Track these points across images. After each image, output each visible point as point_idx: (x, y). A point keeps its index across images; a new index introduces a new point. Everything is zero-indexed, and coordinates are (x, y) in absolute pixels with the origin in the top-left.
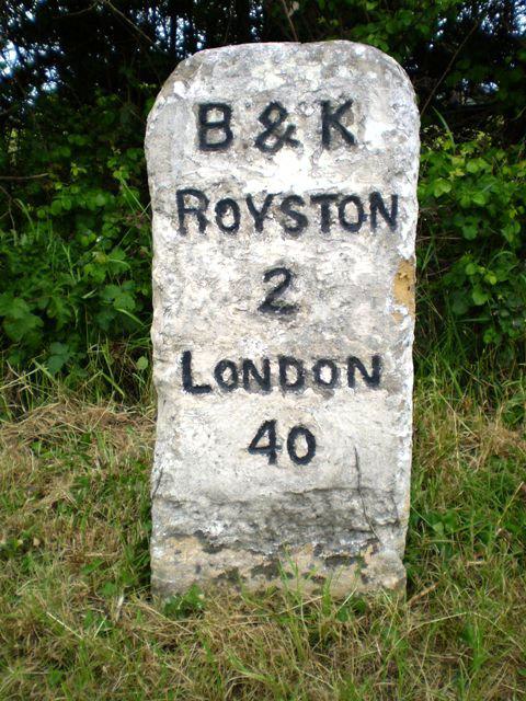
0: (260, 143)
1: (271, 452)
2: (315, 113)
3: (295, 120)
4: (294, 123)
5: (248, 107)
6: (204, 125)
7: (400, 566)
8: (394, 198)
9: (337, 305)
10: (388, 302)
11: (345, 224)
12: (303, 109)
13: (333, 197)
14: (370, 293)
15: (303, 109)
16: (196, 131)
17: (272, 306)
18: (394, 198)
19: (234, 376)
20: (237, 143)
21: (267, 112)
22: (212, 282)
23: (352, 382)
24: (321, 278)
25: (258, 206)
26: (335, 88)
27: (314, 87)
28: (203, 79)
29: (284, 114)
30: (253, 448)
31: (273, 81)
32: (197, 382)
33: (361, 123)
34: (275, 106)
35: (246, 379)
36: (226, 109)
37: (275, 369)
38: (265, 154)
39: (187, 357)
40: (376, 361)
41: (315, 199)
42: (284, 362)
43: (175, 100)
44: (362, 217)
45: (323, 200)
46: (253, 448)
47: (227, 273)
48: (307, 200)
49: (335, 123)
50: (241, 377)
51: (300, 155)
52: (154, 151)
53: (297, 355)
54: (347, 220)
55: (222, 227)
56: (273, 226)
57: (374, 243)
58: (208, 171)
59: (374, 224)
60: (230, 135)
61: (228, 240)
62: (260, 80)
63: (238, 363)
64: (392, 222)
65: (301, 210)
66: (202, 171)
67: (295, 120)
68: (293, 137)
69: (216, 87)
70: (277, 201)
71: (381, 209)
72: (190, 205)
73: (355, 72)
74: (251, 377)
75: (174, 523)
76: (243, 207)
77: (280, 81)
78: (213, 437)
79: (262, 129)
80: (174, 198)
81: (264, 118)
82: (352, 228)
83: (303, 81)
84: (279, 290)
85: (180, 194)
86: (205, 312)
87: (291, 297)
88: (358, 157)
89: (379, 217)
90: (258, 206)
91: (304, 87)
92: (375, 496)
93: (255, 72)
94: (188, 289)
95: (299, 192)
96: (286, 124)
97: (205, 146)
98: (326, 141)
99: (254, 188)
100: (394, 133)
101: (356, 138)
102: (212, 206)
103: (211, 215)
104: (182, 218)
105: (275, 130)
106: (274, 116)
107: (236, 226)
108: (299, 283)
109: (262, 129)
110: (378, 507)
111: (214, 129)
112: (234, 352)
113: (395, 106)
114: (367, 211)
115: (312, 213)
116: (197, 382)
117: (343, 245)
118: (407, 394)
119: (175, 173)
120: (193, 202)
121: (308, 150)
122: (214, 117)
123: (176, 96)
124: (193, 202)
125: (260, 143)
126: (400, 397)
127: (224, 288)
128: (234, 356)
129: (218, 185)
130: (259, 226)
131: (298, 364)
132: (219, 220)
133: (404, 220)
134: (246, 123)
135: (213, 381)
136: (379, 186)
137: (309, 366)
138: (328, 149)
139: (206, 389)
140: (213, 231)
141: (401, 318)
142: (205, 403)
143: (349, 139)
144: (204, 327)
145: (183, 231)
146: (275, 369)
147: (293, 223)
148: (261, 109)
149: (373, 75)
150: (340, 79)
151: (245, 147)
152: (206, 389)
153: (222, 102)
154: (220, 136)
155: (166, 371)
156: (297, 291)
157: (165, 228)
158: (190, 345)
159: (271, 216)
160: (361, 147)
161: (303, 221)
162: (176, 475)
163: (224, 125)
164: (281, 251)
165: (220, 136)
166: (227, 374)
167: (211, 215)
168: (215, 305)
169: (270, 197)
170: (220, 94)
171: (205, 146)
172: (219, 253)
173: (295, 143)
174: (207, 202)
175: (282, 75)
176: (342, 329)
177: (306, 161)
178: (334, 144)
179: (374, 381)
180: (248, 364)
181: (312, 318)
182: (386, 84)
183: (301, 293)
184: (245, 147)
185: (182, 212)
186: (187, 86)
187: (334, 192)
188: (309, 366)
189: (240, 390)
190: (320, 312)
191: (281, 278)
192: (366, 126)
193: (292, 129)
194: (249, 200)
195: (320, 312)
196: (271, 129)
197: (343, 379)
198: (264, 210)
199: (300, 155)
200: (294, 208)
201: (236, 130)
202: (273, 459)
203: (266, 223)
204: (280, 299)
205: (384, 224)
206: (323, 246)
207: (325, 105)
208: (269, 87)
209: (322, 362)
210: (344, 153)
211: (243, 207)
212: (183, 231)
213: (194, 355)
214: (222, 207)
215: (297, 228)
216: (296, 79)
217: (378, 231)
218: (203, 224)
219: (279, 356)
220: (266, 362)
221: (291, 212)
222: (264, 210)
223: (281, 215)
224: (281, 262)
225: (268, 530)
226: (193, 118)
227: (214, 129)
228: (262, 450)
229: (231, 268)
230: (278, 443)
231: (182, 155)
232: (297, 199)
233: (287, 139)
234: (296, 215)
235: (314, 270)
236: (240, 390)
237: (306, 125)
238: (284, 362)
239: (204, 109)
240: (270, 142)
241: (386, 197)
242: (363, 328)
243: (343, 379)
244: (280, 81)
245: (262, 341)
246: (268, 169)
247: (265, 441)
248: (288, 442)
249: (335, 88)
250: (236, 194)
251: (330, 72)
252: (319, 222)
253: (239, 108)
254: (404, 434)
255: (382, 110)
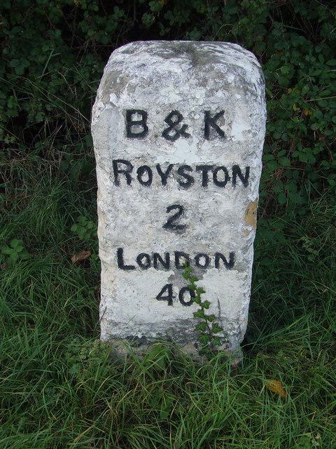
0: (165, 134)
1: (170, 300)
2: (200, 118)
3: (187, 121)
4: (186, 123)
5: (158, 113)
6: (129, 122)
7: (241, 354)
8: (248, 169)
9: (210, 226)
10: (241, 225)
11: (216, 182)
12: (193, 115)
13: (209, 167)
14: (230, 220)
15: (193, 115)
16: (124, 126)
17: (170, 225)
18: (248, 169)
19: (148, 261)
20: (150, 135)
21: (171, 116)
22: (135, 212)
23: (217, 265)
24: (201, 211)
25: (164, 170)
26: (214, 103)
27: (201, 102)
28: (129, 95)
29: (180, 118)
30: (159, 298)
31: (174, 98)
32: (126, 264)
33: (230, 125)
34: (175, 113)
35: (155, 262)
36: (144, 114)
37: (172, 258)
38: (168, 141)
39: (120, 252)
40: (232, 255)
41: (199, 168)
42: (178, 255)
43: (111, 107)
44: (227, 178)
45: (204, 169)
46: (159, 298)
47: (144, 207)
48: (194, 169)
49: (212, 125)
50: (152, 262)
51: (190, 143)
52: (97, 135)
53: (186, 251)
54: (218, 180)
55: (141, 182)
56: (172, 182)
57: (234, 194)
58: (134, 150)
59: (234, 182)
60: (146, 129)
61: (145, 189)
62: (165, 96)
63: (150, 255)
64: (245, 181)
65: (190, 174)
66: (129, 150)
67: (187, 121)
68: (186, 132)
69: (137, 100)
70: (175, 168)
71: (239, 175)
72: (121, 169)
73: (227, 94)
74: (158, 261)
75: (114, 333)
76: (155, 171)
77: (179, 98)
78: (136, 292)
79: (166, 126)
80: (111, 164)
81: (168, 120)
82: (221, 185)
83: (194, 98)
84: (176, 216)
85: (115, 163)
86: (131, 228)
87: (183, 221)
88: (226, 145)
89: (238, 179)
90: (164, 170)
91: (194, 103)
92: (227, 320)
93: (163, 91)
94: (121, 215)
95: (188, 164)
96: (182, 124)
97: (130, 135)
98: (207, 135)
99: (161, 160)
100: (249, 131)
101: (226, 133)
102: (135, 170)
103: (134, 175)
104: (116, 175)
105: (174, 127)
106: (174, 119)
107: (150, 181)
108: (188, 214)
109: (166, 126)
110: (229, 327)
111: (135, 124)
112: (148, 249)
113: (251, 115)
114: (231, 175)
115: (197, 176)
116: (126, 264)
117: (216, 194)
118: (249, 272)
119: (111, 150)
120: (123, 167)
121: (195, 140)
122: (136, 118)
123: (112, 104)
124: (123, 167)
125: (165, 134)
126: (245, 274)
127: (143, 216)
128: (149, 251)
129: (139, 158)
130: (164, 182)
131: (186, 256)
132: (139, 178)
133: (253, 179)
134: (156, 122)
135: (136, 264)
136: (239, 162)
137: (192, 257)
138: (208, 139)
139: (132, 268)
140: (135, 183)
141: (247, 232)
142: (131, 275)
143: (222, 134)
144: (129, 236)
145: (117, 183)
146: (172, 258)
147: (185, 181)
148: (166, 115)
149: (238, 97)
150: (217, 98)
151: (156, 136)
152: (132, 268)
153: (141, 109)
154: (140, 129)
155: (107, 256)
156: (187, 218)
157: (106, 180)
158: (122, 245)
159: (172, 176)
160: (228, 139)
161: (191, 180)
162: (115, 310)
163: (143, 123)
164: (177, 196)
165: (140, 129)
166: (144, 260)
167: (134, 175)
168: (137, 224)
169: (171, 166)
170: (140, 105)
171: (130, 135)
172: (139, 196)
173: (187, 136)
174: (132, 167)
175: (180, 94)
176: (213, 238)
177: (194, 147)
178: (211, 137)
179: (230, 265)
180: (156, 256)
181: (195, 233)
182: (247, 102)
183: (189, 219)
184: (156, 136)
185: (116, 172)
186: (118, 97)
187: (211, 164)
188: (192, 257)
189: (152, 268)
190: (199, 229)
191: (177, 210)
192: (232, 127)
193: (185, 126)
194: (158, 167)
195: (199, 229)
196: (172, 125)
197: (212, 263)
198: (168, 172)
199: (190, 143)
200: (186, 172)
201: (150, 126)
202: (170, 303)
203: (168, 180)
204: (177, 221)
205: (240, 183)
206: (203, 194)
207: (207, 114)
208: (172, 101)
209: (200, 255)
210: (218, 143)
211: (155, 171)
212: (117, 183)
213: (124, 250)
214: (141, 171)
215: (187, 183)
216: (189, 97)
217: (237, 186)
218: (129, 180)
219: (175, 252)
220: (167, 255)
221: (184, 176)
222: (168, 172)
223: (178, 176)
224: (178, 202)
225: (167, 336)
226: (123, 119)
227: (135, 124)
228: (164, 299)
229: (146, 205)
230: (173, 295)
231: (115, 140)
232: (188, 168)
233: (183, 133)
234: (187, 176)
235: (197, 208)
236: (152, 268)
237: (195, 125)
238: (178, 255)
239: (129, 113)
240: (172, 134)
241: (242, 168)
242: (226, 239)
243: (212, 263)
244: (179, 98)
245: (167, 243)
246: (171, 150)
247: (166, 294)
248: (180, 294)
249: (214, 103)
250: (149, 163)
251: (211, 93)
252: (201, 180)
253: (152, 114)
254: (246, 291)
255: (243, 117)
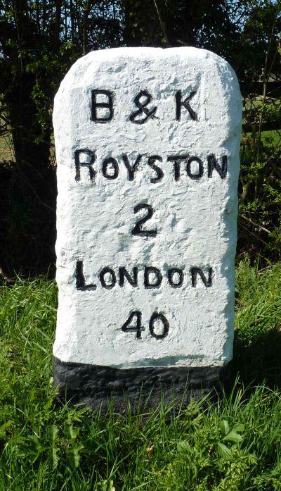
13: (184, 157)
25: (132, 163)
30: (125, 328)
32: (87, 283)
34: (144, 93)
45: (174, 159)
46: (125, 328)
72: (83, 157)
81: (136, 100)
90: (132, 163)
103: (97, 166)
107: (115, 176)
111: (100, 105)
115: (166, 167)
116: (87, 283)
132: (104, 170)
135: (97, 281)
139: (92, 287)
146: (141, 274)
152: (92, 287)
153: (107, 89)
158: (81, 257)
163: (110, 105)
194: (125, 158)
196: (142, 108)
214: (109, 160)
218: (92, 173)
247: (133, 324)
